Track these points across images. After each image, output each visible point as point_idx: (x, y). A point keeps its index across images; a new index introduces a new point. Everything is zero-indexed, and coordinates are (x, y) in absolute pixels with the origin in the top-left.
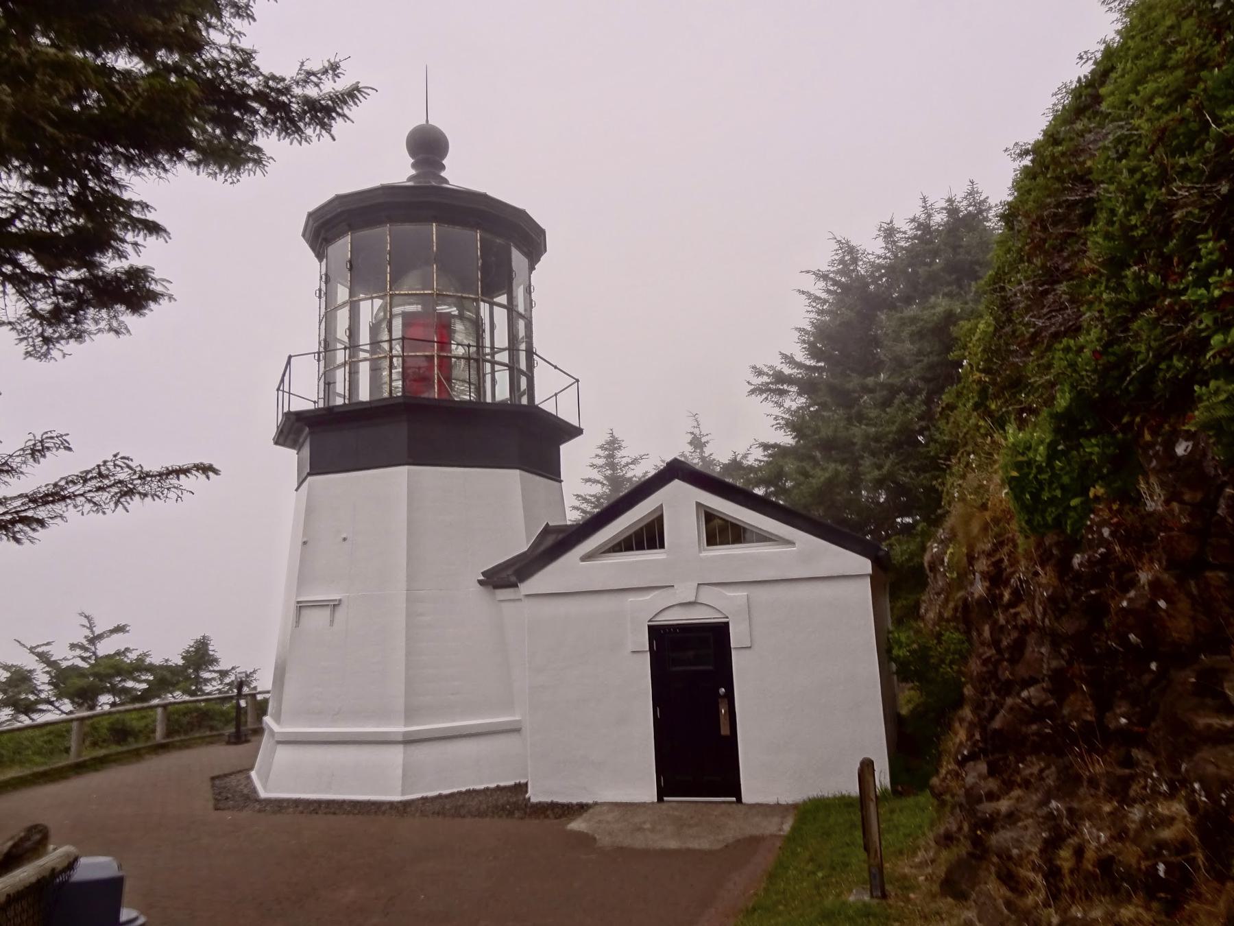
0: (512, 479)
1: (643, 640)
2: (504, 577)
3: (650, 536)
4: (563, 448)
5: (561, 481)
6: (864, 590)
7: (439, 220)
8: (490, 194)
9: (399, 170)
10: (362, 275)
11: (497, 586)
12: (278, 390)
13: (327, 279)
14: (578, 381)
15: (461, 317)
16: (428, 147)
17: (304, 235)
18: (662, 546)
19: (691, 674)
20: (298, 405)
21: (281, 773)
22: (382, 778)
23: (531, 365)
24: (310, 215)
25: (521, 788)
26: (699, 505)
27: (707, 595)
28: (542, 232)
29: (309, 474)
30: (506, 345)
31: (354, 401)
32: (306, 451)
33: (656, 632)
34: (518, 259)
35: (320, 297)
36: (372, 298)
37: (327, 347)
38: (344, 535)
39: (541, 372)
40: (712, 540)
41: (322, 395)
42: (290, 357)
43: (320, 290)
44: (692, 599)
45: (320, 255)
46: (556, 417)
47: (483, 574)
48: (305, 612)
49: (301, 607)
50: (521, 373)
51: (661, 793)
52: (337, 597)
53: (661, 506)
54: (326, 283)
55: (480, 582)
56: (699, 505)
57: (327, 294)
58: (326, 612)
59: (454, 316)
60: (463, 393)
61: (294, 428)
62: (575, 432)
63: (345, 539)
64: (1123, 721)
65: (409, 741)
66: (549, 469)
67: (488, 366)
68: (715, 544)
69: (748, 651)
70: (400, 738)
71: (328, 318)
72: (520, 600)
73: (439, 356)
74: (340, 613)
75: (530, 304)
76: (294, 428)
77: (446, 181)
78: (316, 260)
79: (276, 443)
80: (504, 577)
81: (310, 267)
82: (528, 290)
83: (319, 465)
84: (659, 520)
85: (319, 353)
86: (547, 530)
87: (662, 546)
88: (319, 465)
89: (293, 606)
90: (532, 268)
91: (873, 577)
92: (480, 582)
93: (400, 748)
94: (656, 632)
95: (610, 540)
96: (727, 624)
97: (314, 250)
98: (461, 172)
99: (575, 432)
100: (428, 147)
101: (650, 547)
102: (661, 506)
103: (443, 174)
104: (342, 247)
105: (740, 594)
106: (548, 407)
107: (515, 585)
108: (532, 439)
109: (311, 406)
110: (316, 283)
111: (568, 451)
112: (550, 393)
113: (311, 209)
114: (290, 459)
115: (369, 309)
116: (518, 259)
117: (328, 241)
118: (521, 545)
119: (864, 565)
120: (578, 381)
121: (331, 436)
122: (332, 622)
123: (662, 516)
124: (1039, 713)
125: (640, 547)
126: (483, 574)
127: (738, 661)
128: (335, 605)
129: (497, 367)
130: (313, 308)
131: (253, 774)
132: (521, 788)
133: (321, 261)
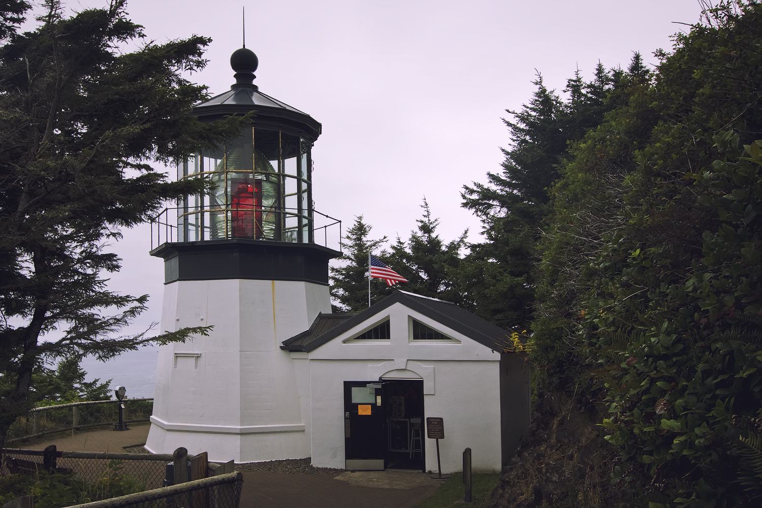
0: (300, 287)
2: (293, 346)
3: (382, 331)
11: (291, 351)
14: (340, 222)
18: (389, 338)
27: (412, 366)
30: (296, 191)
38: (202, 317)
40: (416, 337)
44: (404, 368)
47: (283, 343)
50: (306, 215)
52: (199, 353)
55: (281, 347)
58: (193, 360)
63: (202, 320)
65: (242, 433)
69: (434, 396)
74: (201, 361)
87: (389, 338)
89: (172, 357)
91: (501, 362)
92: (281, 347)
93: (239, 437)
95: (358, 333)
101: (382, 338)
105: (431, 366)
120: (340, 222)
122: (196, 367)
125: (377, 338)
126: (283, 343)
128: (198, 357)
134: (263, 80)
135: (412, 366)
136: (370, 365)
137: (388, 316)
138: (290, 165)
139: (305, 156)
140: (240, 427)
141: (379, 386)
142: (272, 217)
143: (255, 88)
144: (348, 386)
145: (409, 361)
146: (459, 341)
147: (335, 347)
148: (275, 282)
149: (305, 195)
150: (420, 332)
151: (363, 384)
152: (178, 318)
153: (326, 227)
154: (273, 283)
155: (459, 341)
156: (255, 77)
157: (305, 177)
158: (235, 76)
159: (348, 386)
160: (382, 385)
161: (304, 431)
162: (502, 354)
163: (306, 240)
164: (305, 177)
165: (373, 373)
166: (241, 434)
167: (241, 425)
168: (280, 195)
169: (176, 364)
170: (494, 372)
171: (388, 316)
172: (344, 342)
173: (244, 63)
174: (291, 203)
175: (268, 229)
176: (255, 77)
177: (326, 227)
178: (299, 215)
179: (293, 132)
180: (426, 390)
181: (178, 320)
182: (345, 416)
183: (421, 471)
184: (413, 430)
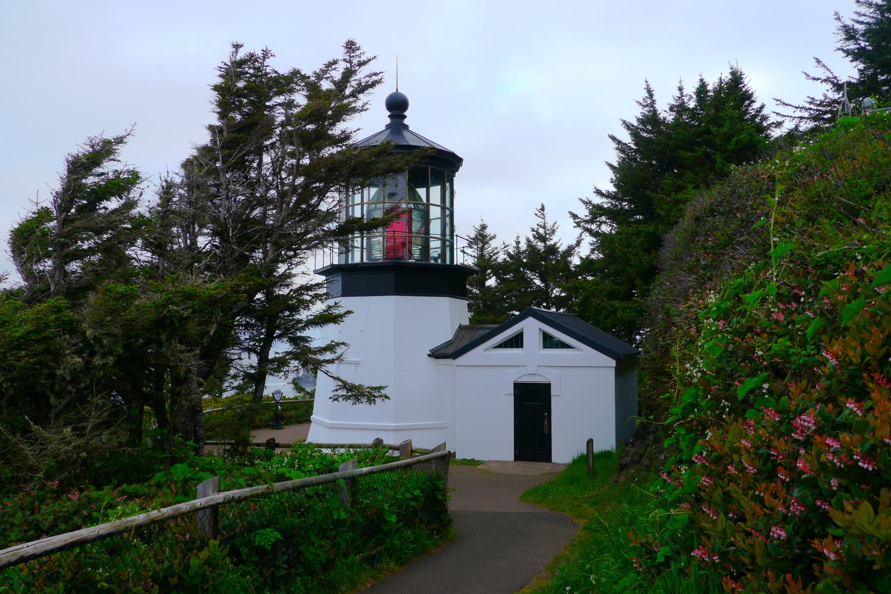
1: (511, 390)
3: (517, 342)
6: (612, 373)
18: (522, 347)
19: (532, 406)
33: (518, 386)
51: (517, 457)
55: (429, 355)
87: (522, 347)
91: (616, 368)
92: (429, 355)
94: (518, 386)
96: (549, 385)
101: (517, 347)
103: (406, 122)
105: (557, 371)
119: (612, 363)
125: (511, 347)
127: (554, 401)
134: (411, 119)
138: (435, 191)
139: (448, 185)
142: (419, 241)
143: (406, 127)
146: (581, 350)
149: (448, 220)
150: (549, 342)
156: (405, 117)
157: (448, 204)
158: (389, 116)
162: (618, 361)
163: (448, 262)
164: (448, 204)
166: (395, 430)
168: (426, 221)
170: (610, 376)
172: (487, 349)
173: (397, 106)
174: (435, 228)
175: (416, 251)
176: (405, 117)
179: (440, 166)
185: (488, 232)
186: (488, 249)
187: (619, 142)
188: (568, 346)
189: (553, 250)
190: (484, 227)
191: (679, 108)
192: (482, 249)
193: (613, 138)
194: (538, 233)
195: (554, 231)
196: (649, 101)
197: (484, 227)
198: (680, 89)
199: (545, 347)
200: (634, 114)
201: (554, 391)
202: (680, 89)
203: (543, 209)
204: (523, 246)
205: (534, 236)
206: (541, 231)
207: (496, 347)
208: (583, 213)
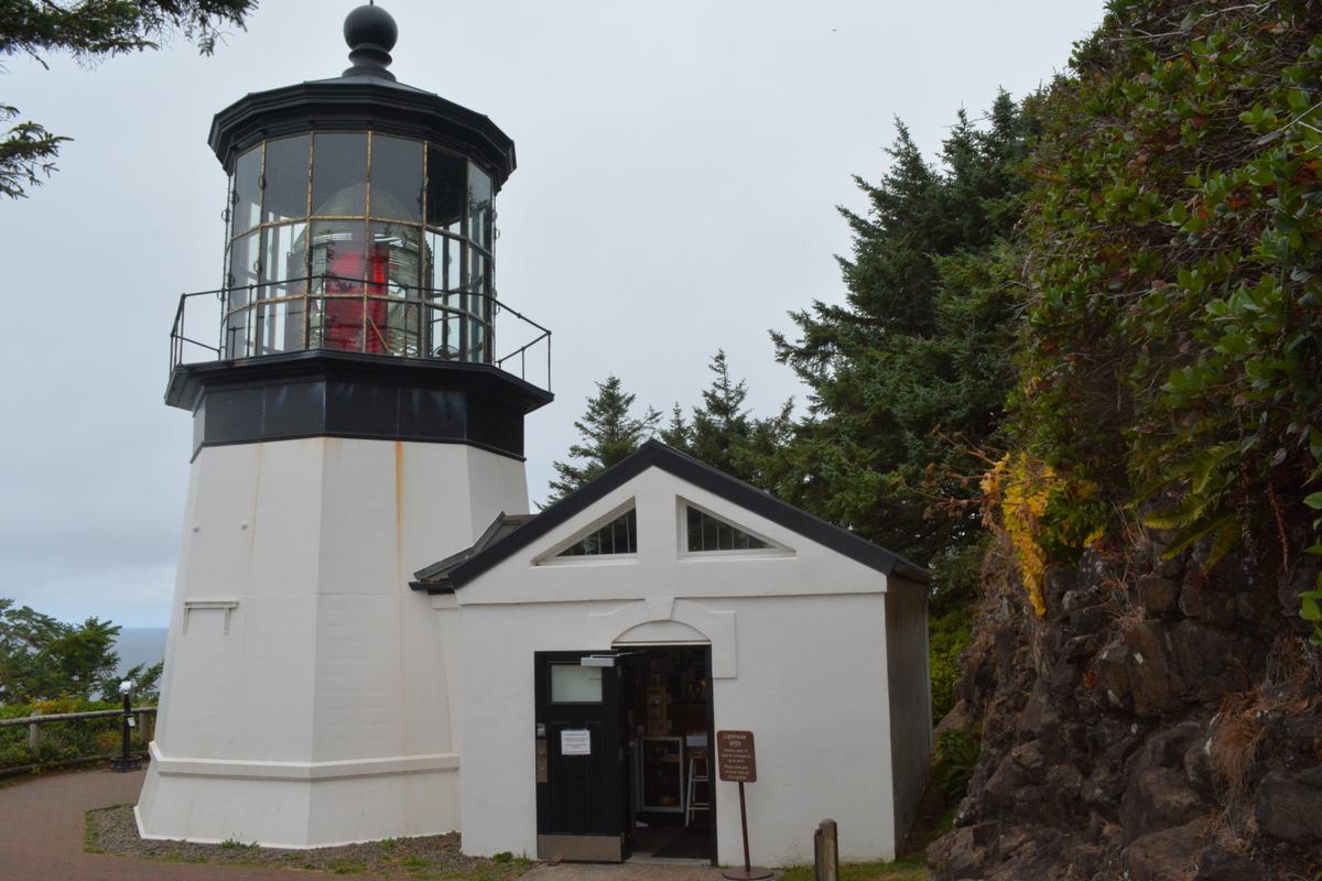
2: (442, 581)
3: (619, 536)
4: (526, 417)
5: (524, 460)
6: (877, 612)
7: (378, 129)
8: (440, 95)
9: (332, 61)
10: (278, 197)
12: (172, 335)
13: (235, 198)
14: (549, 333)
15: (404, 250)
16: (371, 36)
17: (209, 143)
18: (634, 550)
20: (194, 356)
21: (166, 810)
22: (286, 824)
23: (489, 314)
24: (217, 117)
25: (455, 838)
26: (680, 499)
27: (685, 612)
28: (509, 144)
29: (205, 445)
31: (259, 354)
32: (202, 413)
34: (477, 178)
35: (227, 220)
36: (292, 223)
37: (232, 286)
38: (244, 523)
39: (501, 321)
41: (224, 344)
42: (184, 297)
43: (228, 211)
44: (667, 617)
45: (229, 168)
46: (522, 381)
48: (195, 616)
49: (190, 608)
53: (633, 498)
54: (234, 203)
55: (414, 586)
56: (680, 499)
57: (235, 213)
58: (220, 617)
59: (394, 247)
60: (405, 349)
61: (188, 384)
62: (542, 398)
63: (244, 527)
64: (1098, 791)
65: (317, 779)
66: (510, 444)
67: (438, 314)
68: (699, 549)
70: (307, 776)
71: (234, 247)
72: (454, 609)
73: (369, 299)
75: (490, 235)
76: (188, 384)
77: (391, 77)
78: (224, 173)
79: (169, 402)
80: (442, 581)
81: (215, 181)
82: (490, 216)
83: (215, 435)
84: (632, 515)
85: (223, 291)
86: (502, 521)
87: (634, 550)
88: (215, 435)
89: (182, 607)
90: (496, 188)
92: (414, 586)
93: (308, 787)
95: (569, 539)
96: (709, 647)
97: (222, 162)
98: (408, 68)
99: (542, 398)
100: (371, 36)
102: (633, 498)
104: (254, 159)
105: (726, 612)
106: (511, 367)
107: (451, 591)
108: (491, 409)
109: (212, 357)
110: (221, 200)
111: (535, 423)
112: (512, 351)
113: (218, 111)
114: (185, 424)
115: (289, 237)
116: (477, 178)
117: (237, 151)
118: (463, 537)
119: (877, 581)
120: (549, 333)
121: (233, 396)
123: (634, 511)
124: (1032, 777)
125: (607, 549)
128: (231, 608)
129: (450, 315)
130: (217, 234)
131: (136, 809)
132: (455, 838)
133: (230, 175)
135: (685, 612)
136: (593, 613)
137: (633, 500)
140: (309, 765)
141: (609, 662)
144: (546, 663)
145: (680, 601)
146: (792, 551)
147: (514, 574)
148: (408, 446)
150: (705, 533)
151: (572, 658)
152: (196, 526)
153: (523, 349)
154: (399, 450)
155: (792, 551)
159: (546, 663)
160: (616, 660)
161: (457, 769)
162: (894, 577)
165: (597, 633)
166: (314, 780)
167: (313, 761)
169: (186, 628)
171: (633, 500)
177: (523, 349)
178: (461, 311)
180: (717, 669)
181: (196, 530)
182: (536, 732)
183: (708, 862)
184: (691, 761)
185: (622, 391)
186: (625, 421)
187: (854, 217)
188: (755, 543)
189: (740, 427)
190: (614, 383)
191: (959, 148)
192: (611, 422)
193: (846, 213)
194: (713, 396)
195: (741, 395)
196: (903, 146)
197: (614, 383)
198: (961, 114)
199: (691, 548)
200: (882, 169)
201: (719, 665)
202: (961, 114)
203: (721, 357)
204: (689, 420)
205: (708, 403)
206: (720, 394)
207: (566, 553)
208: (796, 336)
